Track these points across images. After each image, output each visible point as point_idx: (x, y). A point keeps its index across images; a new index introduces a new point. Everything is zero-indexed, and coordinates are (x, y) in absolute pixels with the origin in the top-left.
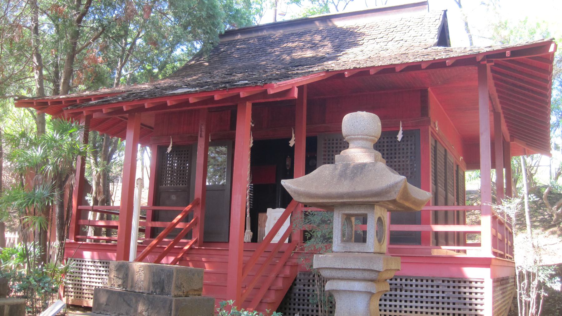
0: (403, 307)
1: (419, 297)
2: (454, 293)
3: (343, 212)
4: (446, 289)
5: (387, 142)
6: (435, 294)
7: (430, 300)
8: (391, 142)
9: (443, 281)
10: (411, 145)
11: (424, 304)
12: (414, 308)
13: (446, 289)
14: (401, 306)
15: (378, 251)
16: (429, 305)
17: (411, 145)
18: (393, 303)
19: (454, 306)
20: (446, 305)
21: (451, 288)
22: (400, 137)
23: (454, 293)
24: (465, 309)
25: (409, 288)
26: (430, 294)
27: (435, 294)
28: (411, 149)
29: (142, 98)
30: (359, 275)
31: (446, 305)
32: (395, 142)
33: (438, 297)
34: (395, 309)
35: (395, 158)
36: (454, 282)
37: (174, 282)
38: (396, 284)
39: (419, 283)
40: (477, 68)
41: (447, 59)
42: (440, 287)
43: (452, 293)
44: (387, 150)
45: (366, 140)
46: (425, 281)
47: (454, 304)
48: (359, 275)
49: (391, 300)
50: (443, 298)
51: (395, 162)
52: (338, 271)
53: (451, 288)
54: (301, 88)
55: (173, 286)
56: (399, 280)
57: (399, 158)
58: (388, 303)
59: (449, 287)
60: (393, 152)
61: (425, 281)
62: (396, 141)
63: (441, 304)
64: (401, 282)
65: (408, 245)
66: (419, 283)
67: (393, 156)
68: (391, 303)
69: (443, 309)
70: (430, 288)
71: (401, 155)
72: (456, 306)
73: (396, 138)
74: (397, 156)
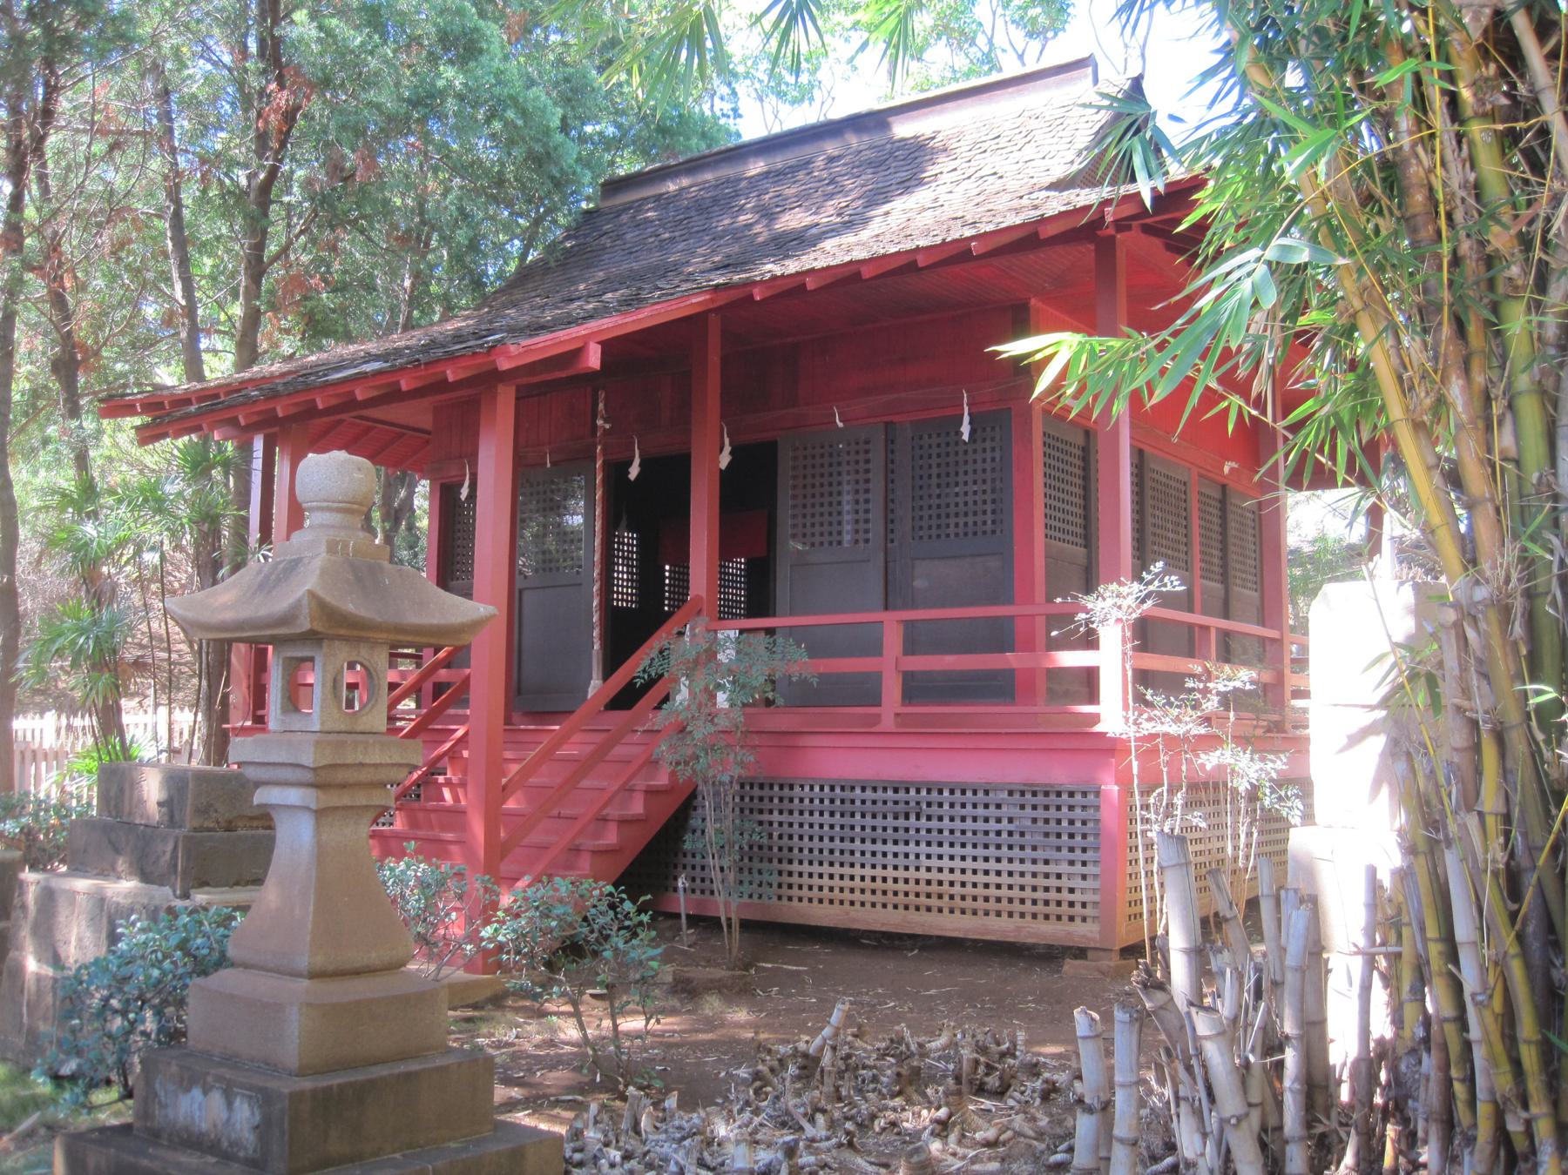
0: (923, 857)
1: (992, 835)
2: (1034, 820)
3: (290, 654)
4: (1015, 812)
5: (939, 445)
6: (992, 825)
7: (980, 838)
8: (948, 444)
9: (1011, 793)
10: (993, 449)
11: (969, 850)
12: (992, 861)
13: (1015, 812)
14: (917, 856)
15: (349, 728)
16: (980, 852)
17: (993, 449)
18: (901, 848)
19: (1035, 855)
20: (1016, 852)
21: (1028, 810)
22: (966, 429)
23: (1034, 820)
24: (1057, 862)
25: (935, 810)
26: (980, 825)
27: (992, 825)
28: (993, 460)
29: (274, 395)
30: (288, 774)
31: (1016, 852)
32: (957, 444)
33: (998, 833)
34: (906, 862)
35: (957, 484)
36: (1046, 794)
37: (189, 802)
38: (907, 803)
39: (869, 794)
40: (1092, 247)
41: (972, 238)
42: (1004, 808)
43: (1029, 823)
44: (939, 465)
45: (338, 510)
46: (969, 794)
47: (1034, 848)
48: (288, 774)
49: (896, 842)
50: (1010, 834)
51: (957, 494)
52: (264, 769)
53: (1028, 810)
54: (607, 346)
55: (189, 810)
56: (913, 792)
57: (966, 483)
58: (890, 848)
59: (1022, 807)
60: (952, 470)
61: (969, 794)
62: (959, 441)
63: (1005, 849)
64: (918, 797)
65: (973, 705)
66: (869, 794)
67: (951, 480)
68: (895, 849)
69: (1010, 860)
70: (980, 811)
71: (970, 478)
72: (1040, 854)
73: (959, 434)
74: (961, 479)
